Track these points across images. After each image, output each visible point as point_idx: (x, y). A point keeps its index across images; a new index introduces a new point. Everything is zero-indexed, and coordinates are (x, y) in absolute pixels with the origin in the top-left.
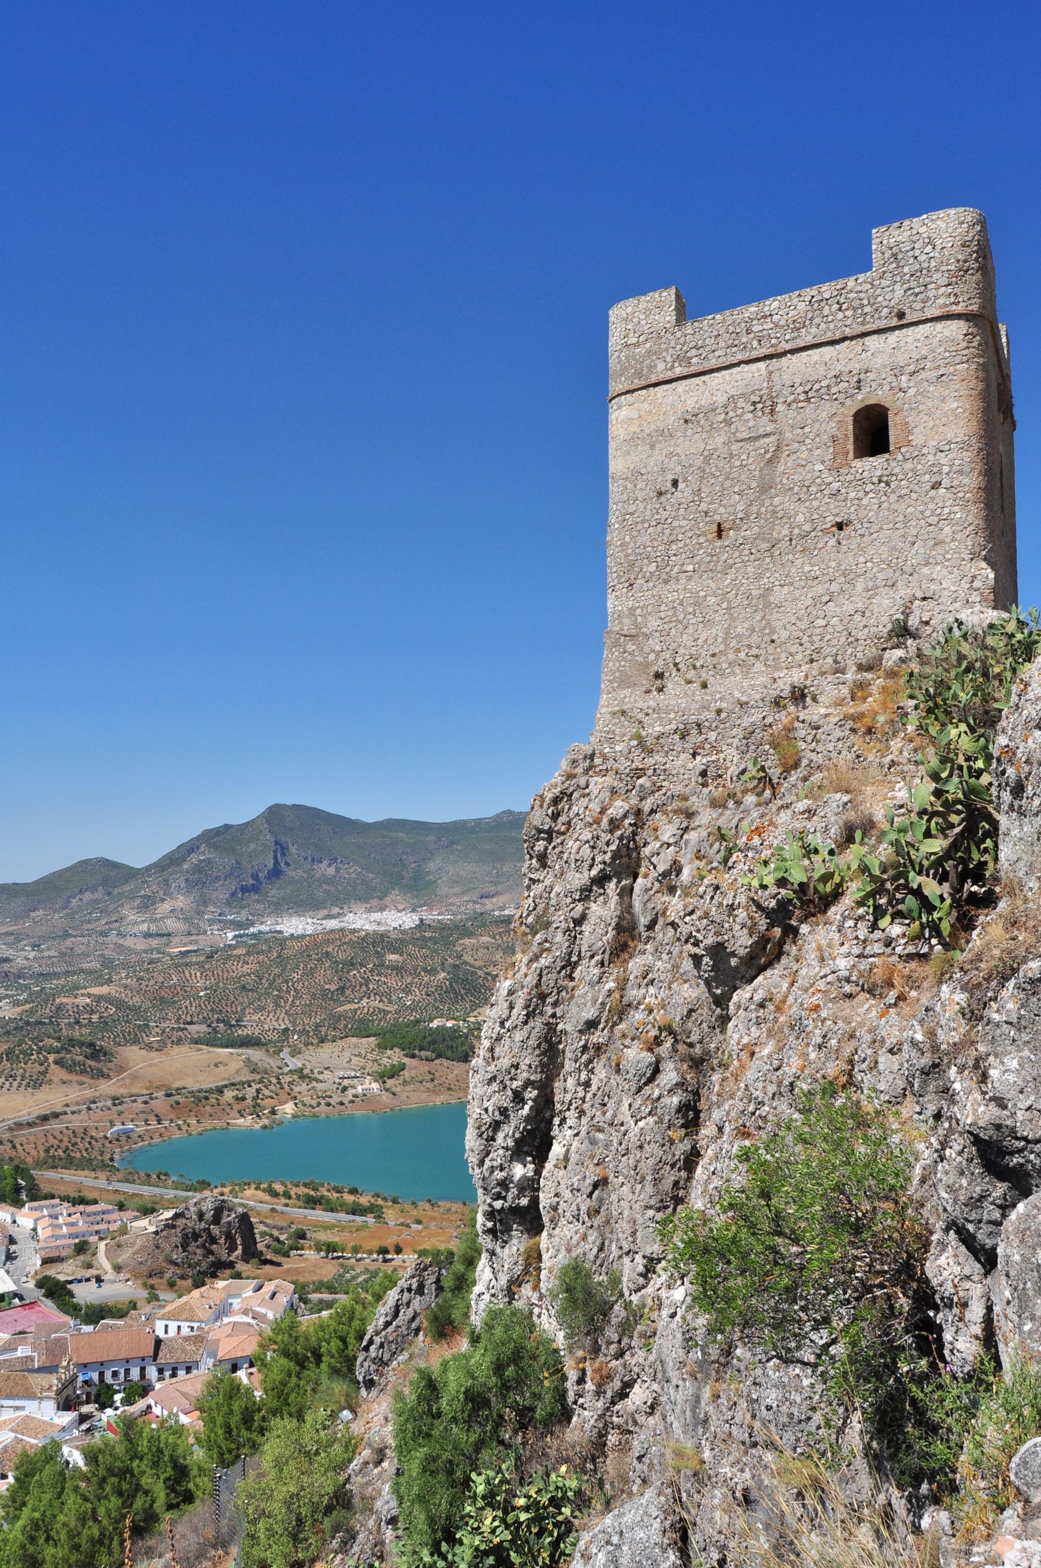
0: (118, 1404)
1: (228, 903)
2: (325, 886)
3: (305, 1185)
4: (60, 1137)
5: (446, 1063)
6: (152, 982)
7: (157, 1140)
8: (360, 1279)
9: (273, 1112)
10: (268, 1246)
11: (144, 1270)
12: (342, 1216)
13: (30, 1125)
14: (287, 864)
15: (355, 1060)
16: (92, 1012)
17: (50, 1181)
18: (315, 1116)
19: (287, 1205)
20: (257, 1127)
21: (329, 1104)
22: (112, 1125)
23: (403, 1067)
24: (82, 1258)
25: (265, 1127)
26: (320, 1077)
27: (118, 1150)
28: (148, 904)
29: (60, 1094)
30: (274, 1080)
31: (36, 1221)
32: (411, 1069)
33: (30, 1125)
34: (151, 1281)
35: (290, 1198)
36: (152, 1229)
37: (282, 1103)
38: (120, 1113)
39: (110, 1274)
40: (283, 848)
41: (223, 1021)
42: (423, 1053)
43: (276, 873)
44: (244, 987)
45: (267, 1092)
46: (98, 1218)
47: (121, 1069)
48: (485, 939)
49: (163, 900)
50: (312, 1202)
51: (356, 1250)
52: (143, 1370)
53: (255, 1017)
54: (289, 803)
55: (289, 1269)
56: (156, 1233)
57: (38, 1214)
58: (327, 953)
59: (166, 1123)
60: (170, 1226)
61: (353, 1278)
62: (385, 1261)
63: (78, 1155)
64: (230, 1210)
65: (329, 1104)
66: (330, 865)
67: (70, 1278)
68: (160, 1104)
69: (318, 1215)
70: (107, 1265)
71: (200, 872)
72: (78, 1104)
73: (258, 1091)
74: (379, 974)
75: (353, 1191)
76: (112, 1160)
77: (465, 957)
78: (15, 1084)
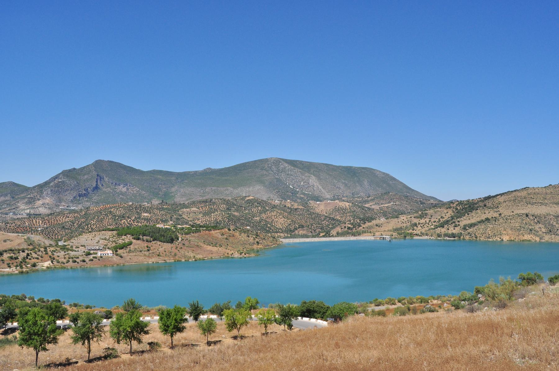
1: (72, 201)
2: (121, 196)
5: (159, 243)
6: (14, 225)
14: (102, 185)
15: (102, 242)
21: (75, 262)
23: (130, 244)
26: (77, 249)
28: (31, 201)
30: (42, 249)
32: (135, 244)
40: (101, 178)
42: (145, 238)
43: (96, 188)
44: (63, 227)
45: (34, 255)
48: (194, 209)
49: (39, 200)
54: (106, 159)
58: (110, 212)
65: (75, 262)
66: (124, 187)
71: (58, 187)
73: (28, 255)
74: (138, 222)
77: (183, 216)
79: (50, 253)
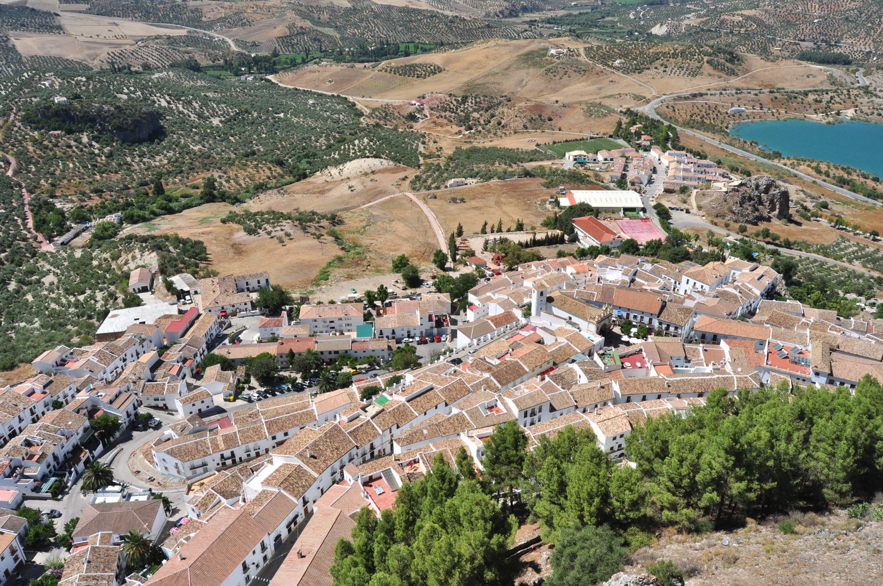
0: (632, 335)
3: (843, 169)
4: (701, 108)
6: (784, 9)
7: (757, 120)
8: (851, 250)
9: (838, 114)
10: (797, 211)
11: (714, 212)
12: (860, 197)
13: (686, 98)
16: (742, 27)
17: (688, 136)
18: (867, 121)
19: (825, 181)
20: (824, 122)
22: (733, 106)
24: (682, 196)
25: (829, 123)
27: (732, 122)
29: (706, 82)
30: (845, 92)
31: (670, 162)
33: (686, 98)
34: (716, 220)
35: (828, 176)
36: (725, 189)
37: (846, 108)
38: (739, 99)
39: (694, 210)
41: (826, 42)
45: (837, 99)
46: (703, 169)
47: (747, 71)
50: (842, 182)
51: (856, 228)
52: (651, 320)
53: (849, 41)
55: (805, 230)
56: (727, 192)
57: (671, 158)
59: (765, 110)
60: (735, 190)
61: (846, 248)
62: (874, 240)
63: (708, 122)
64: (776, 187)
67: (673, 206)
68: (765, 97)
69: (844, 192)
70: (694, 204)
72: (715, 89)
73: (832, 98)
75: (876, 180)
76: (727, 128)
78: (682, 72)
79: (852, 97)
